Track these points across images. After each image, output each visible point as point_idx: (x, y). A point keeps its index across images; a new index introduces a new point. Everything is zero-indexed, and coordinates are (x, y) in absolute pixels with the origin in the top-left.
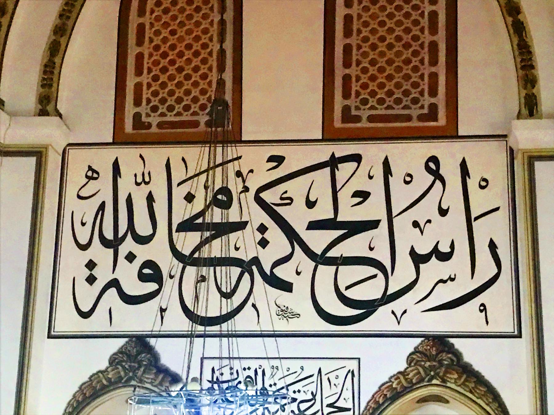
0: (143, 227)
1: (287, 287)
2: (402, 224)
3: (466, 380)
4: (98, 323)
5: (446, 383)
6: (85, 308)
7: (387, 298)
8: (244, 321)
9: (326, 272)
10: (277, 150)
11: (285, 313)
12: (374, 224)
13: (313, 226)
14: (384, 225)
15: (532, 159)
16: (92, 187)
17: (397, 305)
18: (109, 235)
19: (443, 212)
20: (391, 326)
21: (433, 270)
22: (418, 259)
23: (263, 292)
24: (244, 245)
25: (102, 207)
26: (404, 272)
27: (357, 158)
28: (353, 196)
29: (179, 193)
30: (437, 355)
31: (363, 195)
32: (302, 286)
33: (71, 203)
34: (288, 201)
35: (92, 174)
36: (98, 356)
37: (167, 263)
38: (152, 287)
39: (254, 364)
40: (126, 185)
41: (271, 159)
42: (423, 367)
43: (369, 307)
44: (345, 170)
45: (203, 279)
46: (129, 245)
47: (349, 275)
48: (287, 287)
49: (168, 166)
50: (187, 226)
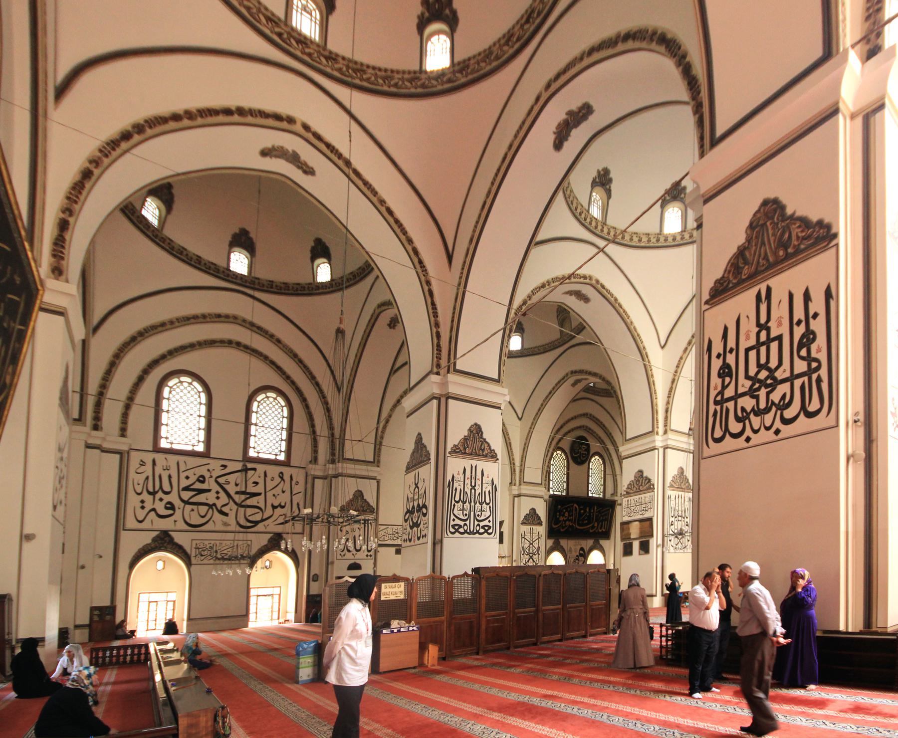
0: (167, 488)
1: (226, 515)
2: (269, 495)
6: (140, 519)
7: (263, 520)
9: (242, 510)
10: (224, 463)
11: (225, 524)
12: (259, 494)
13: (237, 493)
14: (263, 495)
16: (142, 469)
19: (283, 492)
20: (263, 530)
21: (279, 511)
22: (274, 507)
24: (210, 498)
25: (147, 478)
27: (255, 469)
29: (183, 476)
31: (256, 483)
32: (232, 515)
33: (132, 475)
34: (228, 483)
35: (143, 464)
36: (147, 538)
37: (177, 503)
38: (171, 512)
39: (213, 542)
40: (158, 470)
41: (222, 466)
43: (256, 523)
44: (250, 473)
45: (193, 510)
46: (160, 495)
47: (250, 511)
48: (226, 515)
49: (178, 464)
50: (186, 489)
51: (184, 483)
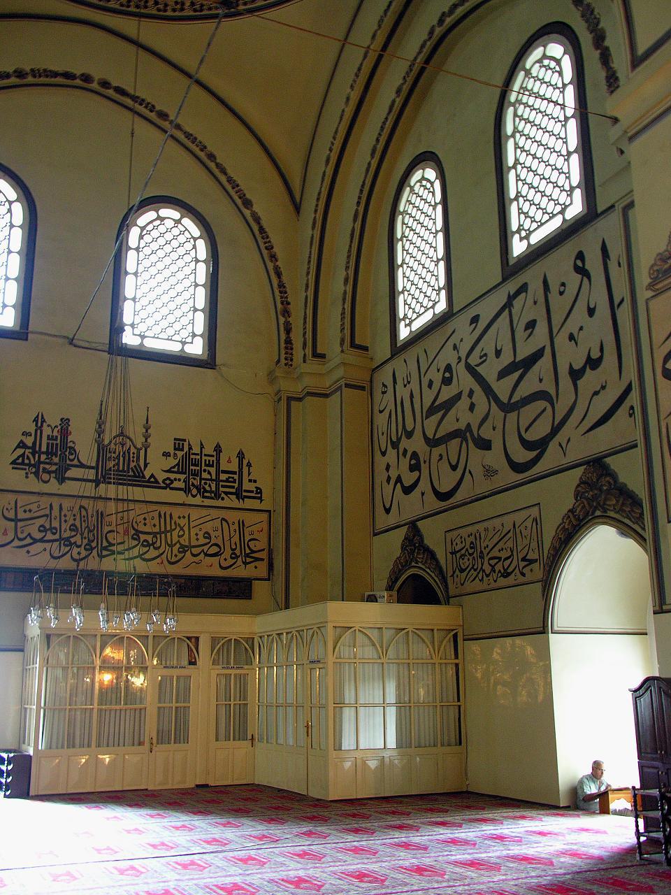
3: (623, 504)
5: (606, 513)
7: (555, 430)
17: (561, 437)
18: (394, 439)
28: (525, 330)
30: (598, 480)
42: (587, 499)
43: (540, 446)
46: (404, 443)
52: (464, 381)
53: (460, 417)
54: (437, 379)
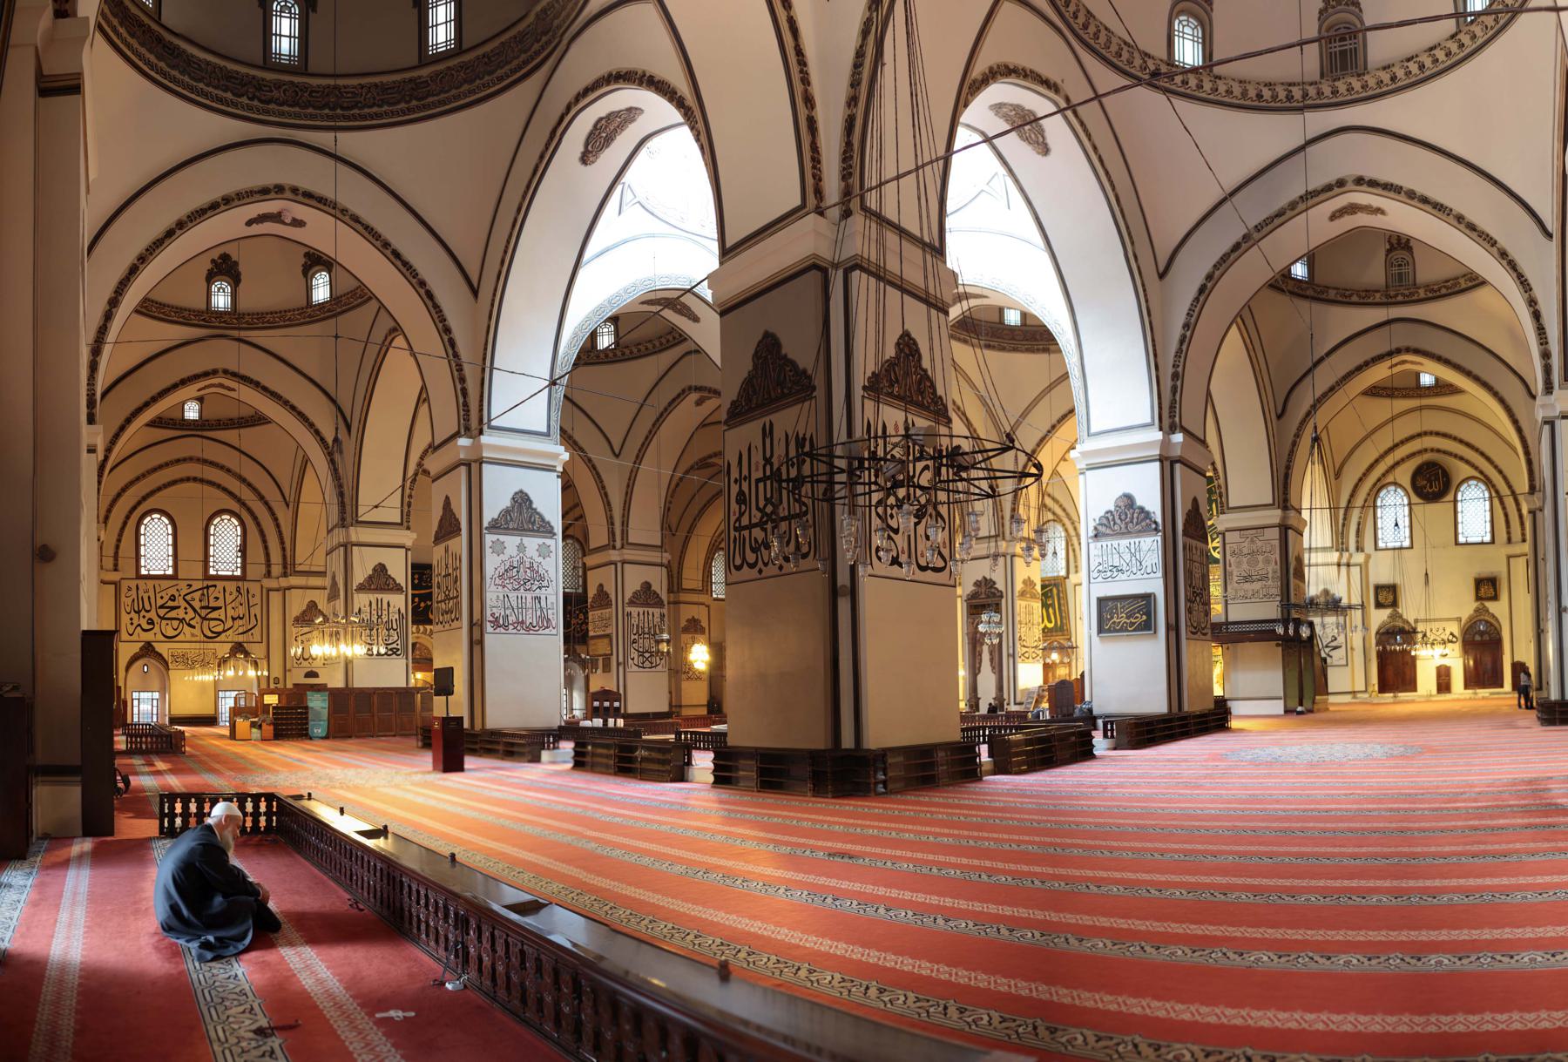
4: (134, 637)
8: (181, 637)
15: (269, 590)
22: (234, 619)
23: (187, 629)
26: (229, 623)
33: (123, 599)
35: (130, 589)
36: (136, 648)
37: (156, 619)
40: (141, 593)
43: (219, 634)
47: (213, 623)
50: (162, 607)
51: (160, 602)
52: (180, 602)
53: (180, 613)
54: (166, 598)
